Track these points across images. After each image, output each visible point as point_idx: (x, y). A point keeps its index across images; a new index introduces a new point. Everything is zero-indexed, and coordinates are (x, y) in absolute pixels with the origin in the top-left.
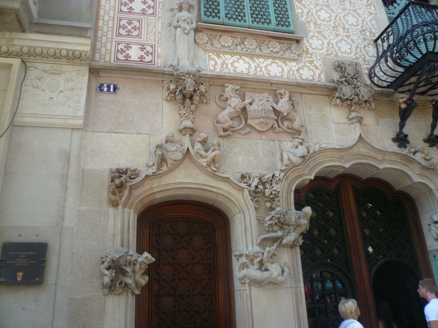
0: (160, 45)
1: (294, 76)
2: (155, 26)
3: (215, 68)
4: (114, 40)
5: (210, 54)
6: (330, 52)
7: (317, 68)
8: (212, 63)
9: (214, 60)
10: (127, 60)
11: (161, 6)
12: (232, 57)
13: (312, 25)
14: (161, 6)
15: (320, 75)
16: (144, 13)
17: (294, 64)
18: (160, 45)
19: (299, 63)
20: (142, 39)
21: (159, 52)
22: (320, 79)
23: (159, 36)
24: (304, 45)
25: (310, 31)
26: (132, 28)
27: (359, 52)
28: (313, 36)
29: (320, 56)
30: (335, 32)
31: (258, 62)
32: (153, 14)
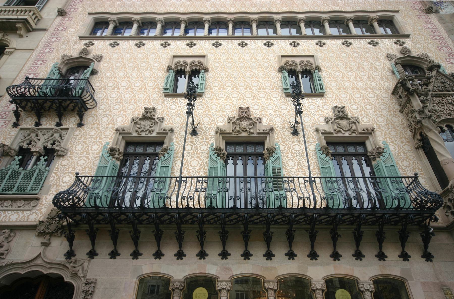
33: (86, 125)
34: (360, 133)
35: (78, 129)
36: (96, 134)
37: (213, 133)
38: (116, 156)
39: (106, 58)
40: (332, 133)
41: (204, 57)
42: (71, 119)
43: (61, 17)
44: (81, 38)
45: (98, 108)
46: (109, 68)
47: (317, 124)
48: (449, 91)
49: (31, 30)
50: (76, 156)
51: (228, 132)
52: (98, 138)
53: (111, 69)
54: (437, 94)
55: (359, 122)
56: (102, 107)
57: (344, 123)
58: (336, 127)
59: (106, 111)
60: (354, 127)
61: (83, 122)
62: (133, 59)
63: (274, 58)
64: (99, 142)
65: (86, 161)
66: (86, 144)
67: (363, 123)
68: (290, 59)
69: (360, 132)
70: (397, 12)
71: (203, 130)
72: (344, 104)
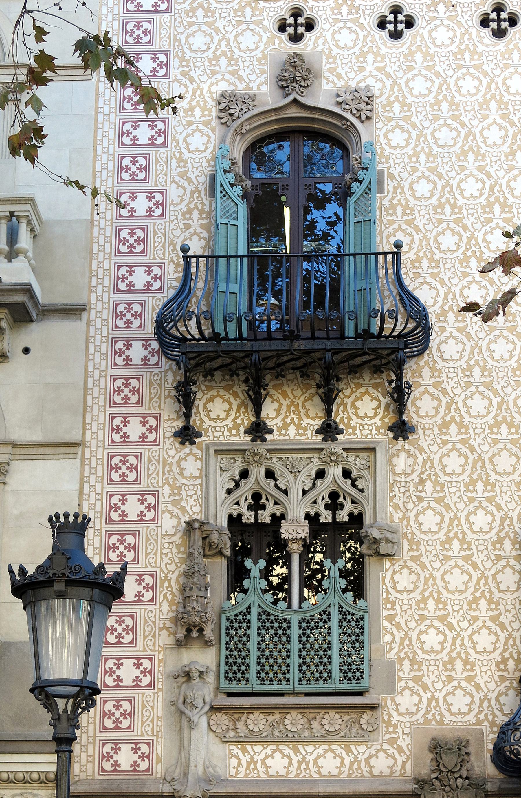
0: (160, 740)
1: (359, 771)
2: (153, 708)
3: (237, 771)
4: (98, 739)
5: (231, 747)
6: (429, 717)
7: (400, 750)
8: (234, 762)
9: (237, 757)
10: (115, 770)
11: (161, 668)
12: (264, 748)
13: (407, 664)
14: (161, 668)
15: (404, 763)
16: (137, 685)
17: (362, 748)
18: (160, 740)
19: (372, 745)
20: (135, 733)
21: (159, 753)
22: (403, 772)
23: (159, 723)
24: (386, 709)
25: (400, 679)
26: (122, 714)
27: (485, 708)
28: (404, 689)
29: (410, 727)
30: (448, 673)
31: (304, 753)
32: (149, 685)
33: (420, 431)
35: (399, 446)
36: (469, 467)
39: (390, 104)
42: (358, 404)
45: (434, 351)
46: (416, 155)
50: (431, 557)
52: (480, 486)
53: (423, 158)
59: (470, 368)
61: (405, 418)
62: (493, 105)
64: (490, 500)
65: (470, 575)
66: (448, 507)
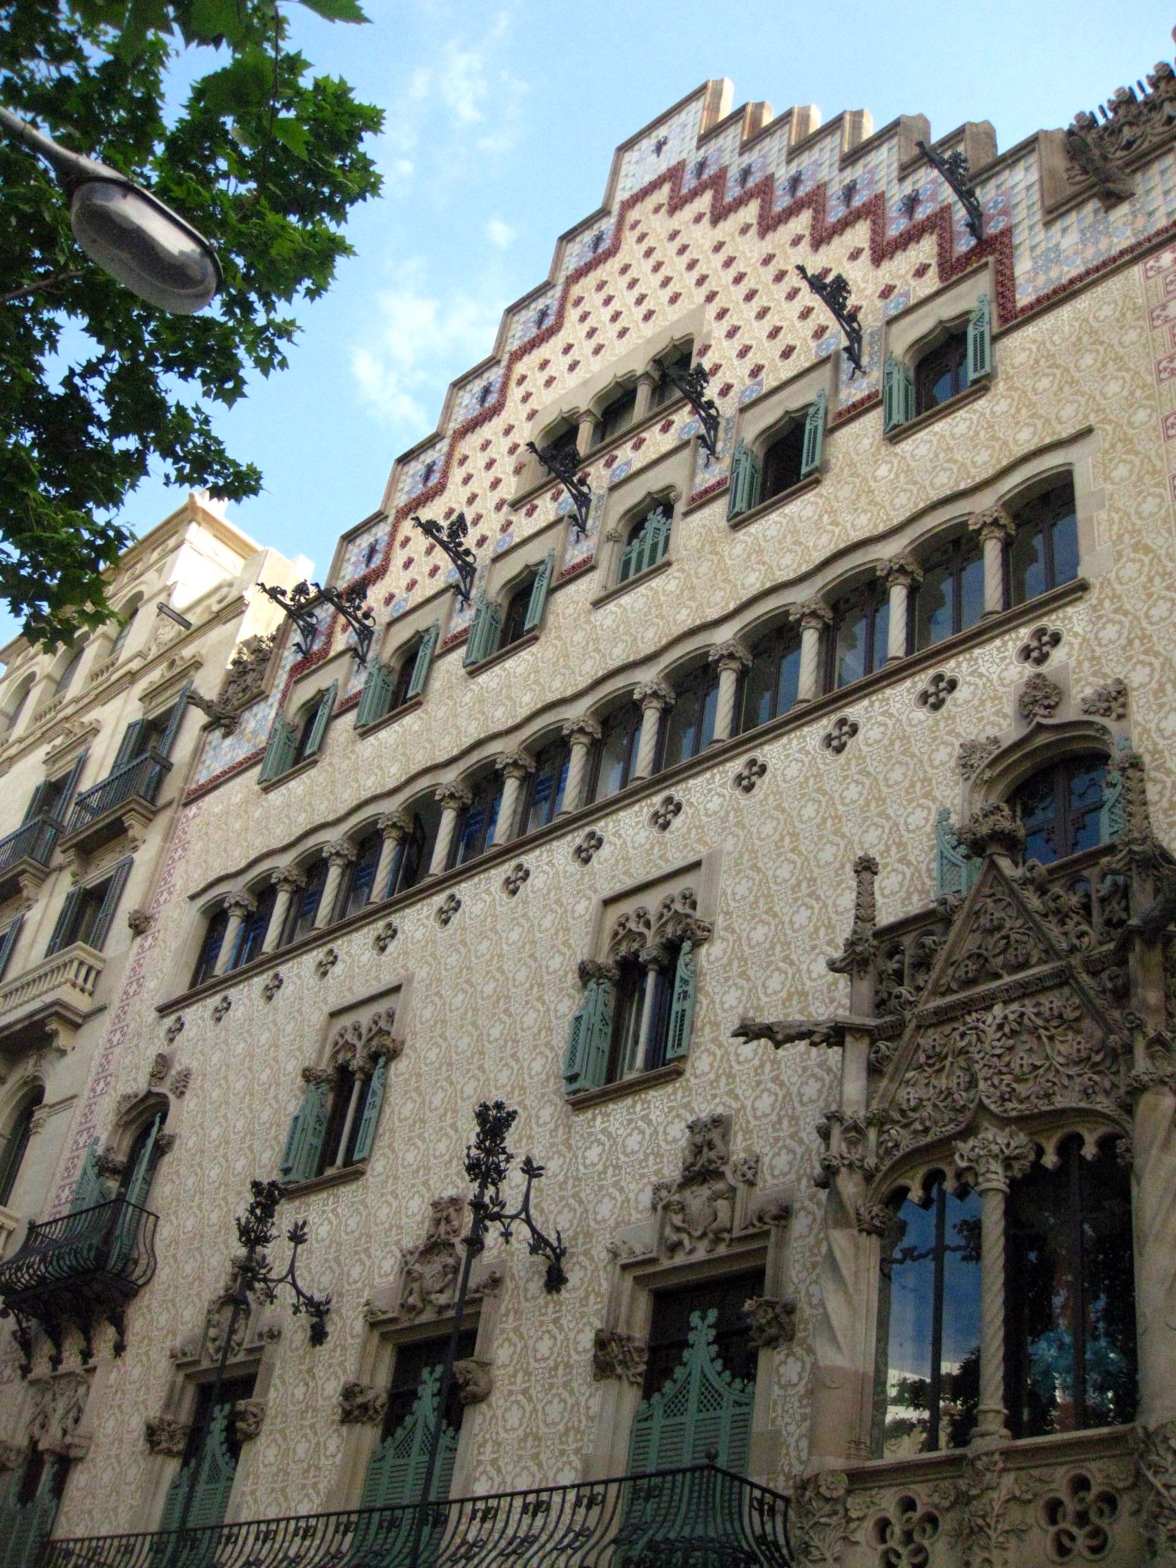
34: (740, 1239)
37: (359, 1326)
38: (164, 1445)
40: (653, 1261)
41: (397, 989)
43: (139, 939)
44: (164, 1010)
47: (629, 1223)
48: (997, 976)
49: (79, 1020)
51: (390, 1315)
54: (937, 1011)
55: (751, 1184)
56: (164, 1274)
57: (697, 1199)
58: (668, 1231)
60: (723, 1218)
63: (587, 917)
67: (770, 1181)
68: (628, 907)
69: (736, 1233)
70: (1089, 431)
71: (341, 1317)
72: (737, 1098)
